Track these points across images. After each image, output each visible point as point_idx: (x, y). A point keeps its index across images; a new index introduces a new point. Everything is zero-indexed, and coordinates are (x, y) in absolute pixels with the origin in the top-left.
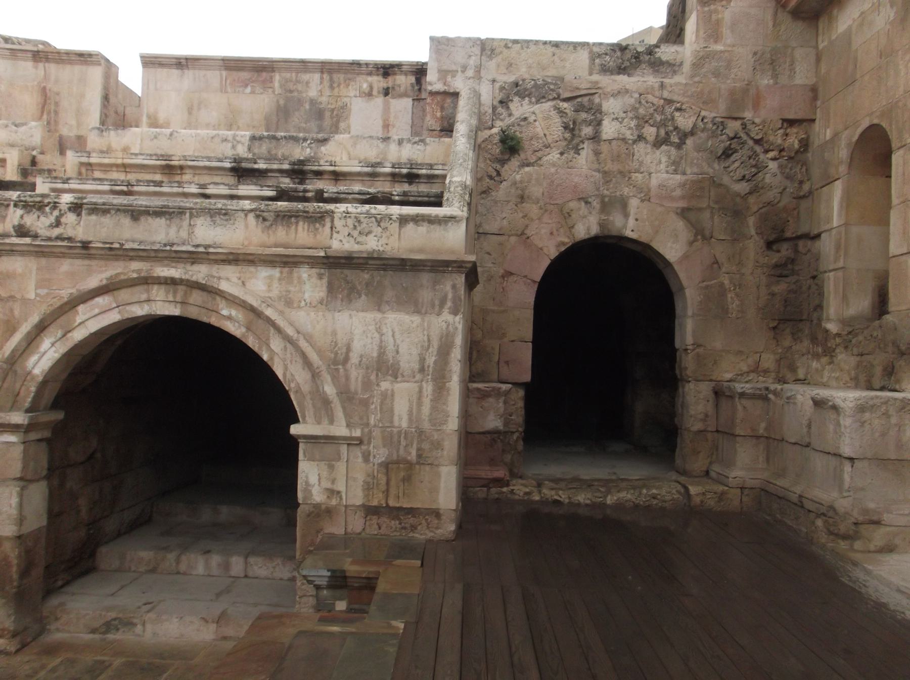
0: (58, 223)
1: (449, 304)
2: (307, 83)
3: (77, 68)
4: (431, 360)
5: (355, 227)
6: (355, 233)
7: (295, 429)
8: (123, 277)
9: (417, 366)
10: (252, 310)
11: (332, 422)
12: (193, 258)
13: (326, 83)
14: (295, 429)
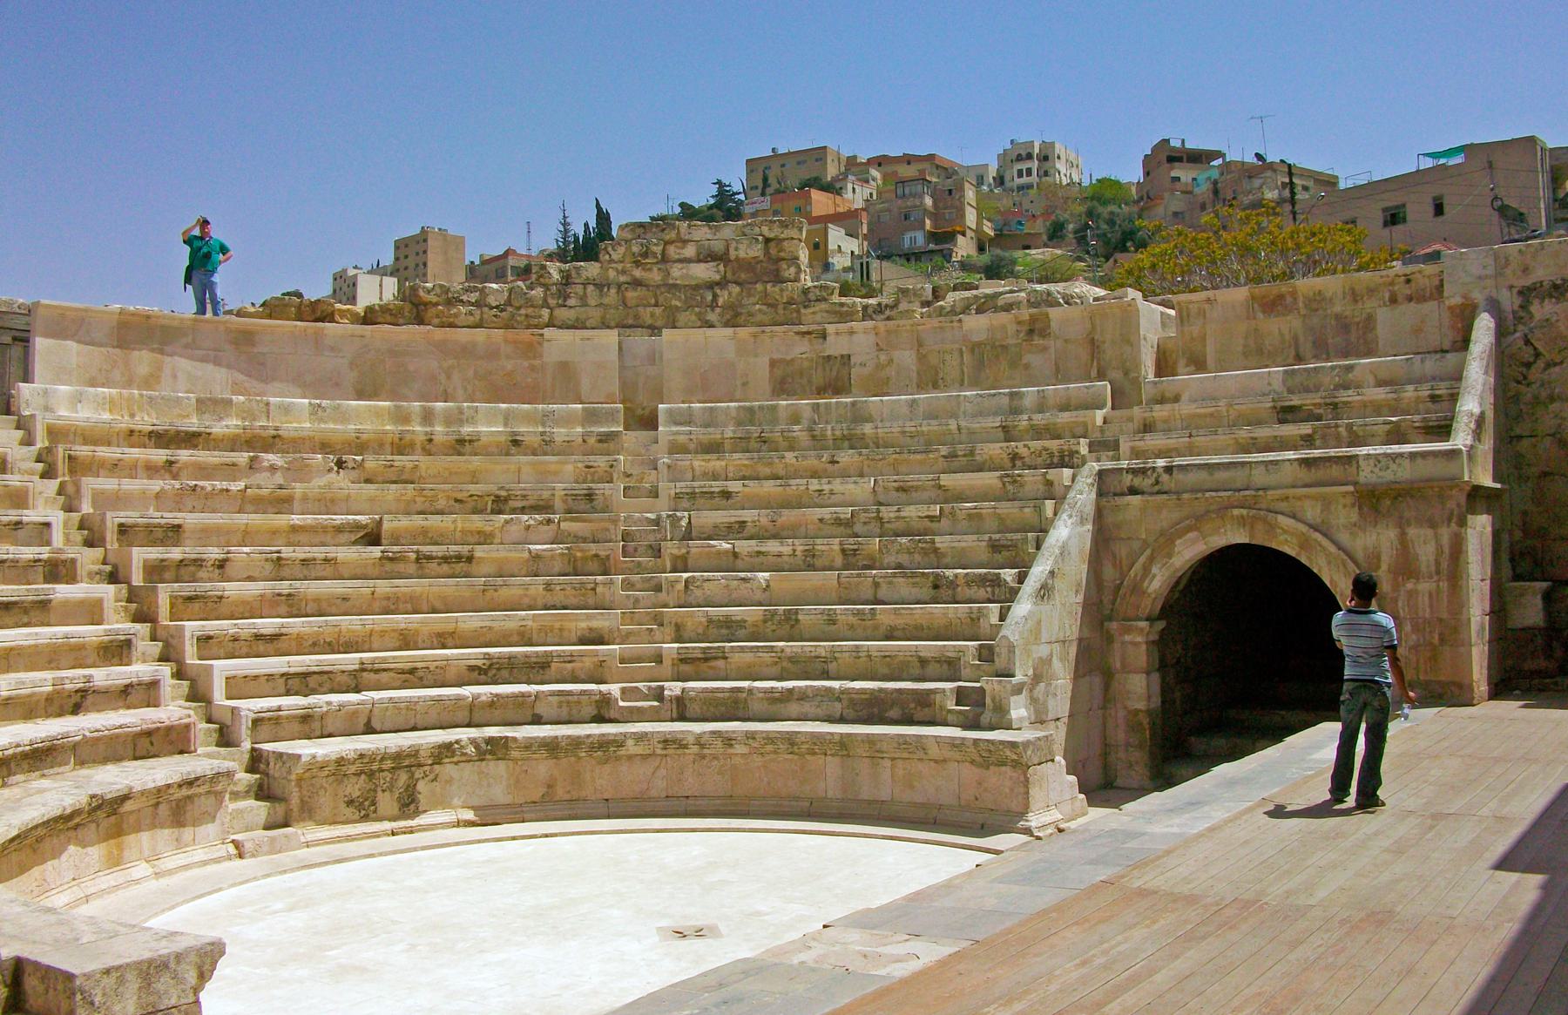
0: (1157, 482)
1: (1455, 520)
4: (1444, 565)
5: (1376, 465)
6: (1377, 470)
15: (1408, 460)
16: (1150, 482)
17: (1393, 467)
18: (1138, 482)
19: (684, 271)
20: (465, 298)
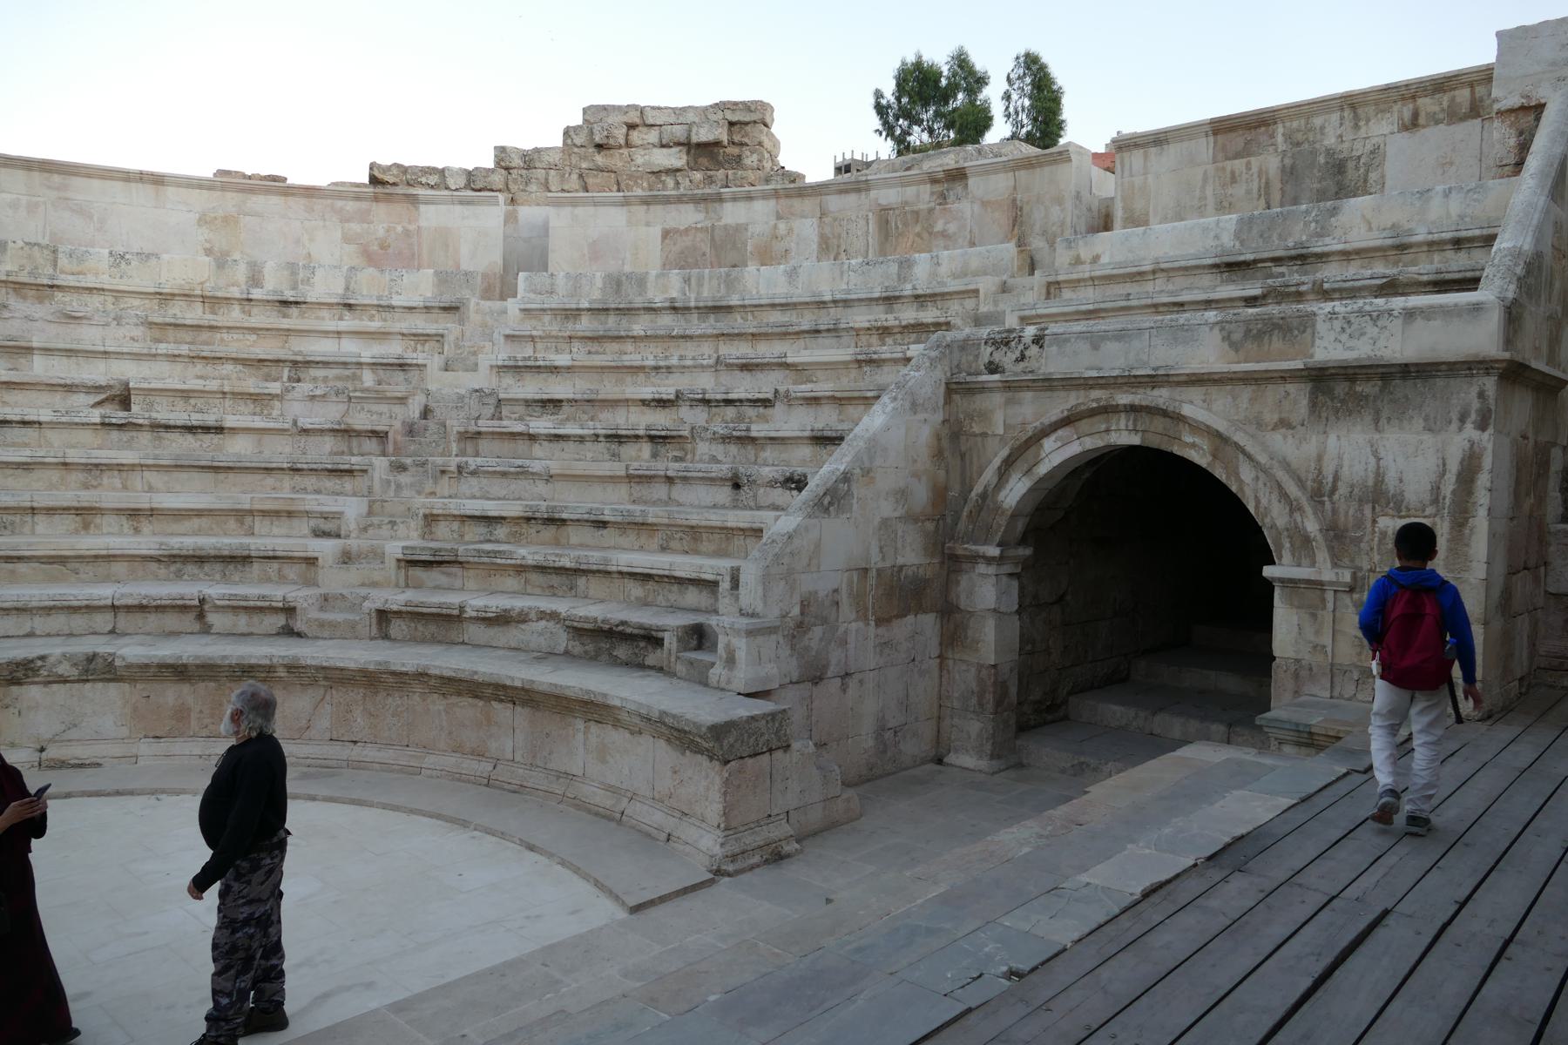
0: (1022, 358)
1: (1473, 416)
2: (1322, 128)
3: (1047, 169)
4: (1448, 487)
7: (1268, 571)
8: (1083, 408)
9: (1427, 497)
10: (1218, 435)
11: (1313, 564)
12: (1154, 381)
13: (1348, 124)
14: (1268, 571)
15: (1399, 322)
16: (1014, 357)
17: (1372, 331)
18: (997, 357)
19: (647, 157)
20: (424, 180)
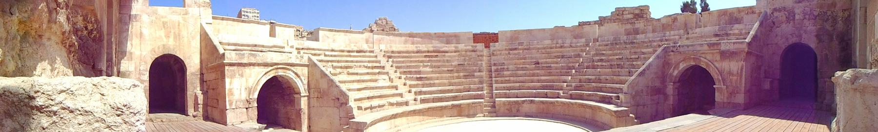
7: (714, 86)
14: (714, 86)
